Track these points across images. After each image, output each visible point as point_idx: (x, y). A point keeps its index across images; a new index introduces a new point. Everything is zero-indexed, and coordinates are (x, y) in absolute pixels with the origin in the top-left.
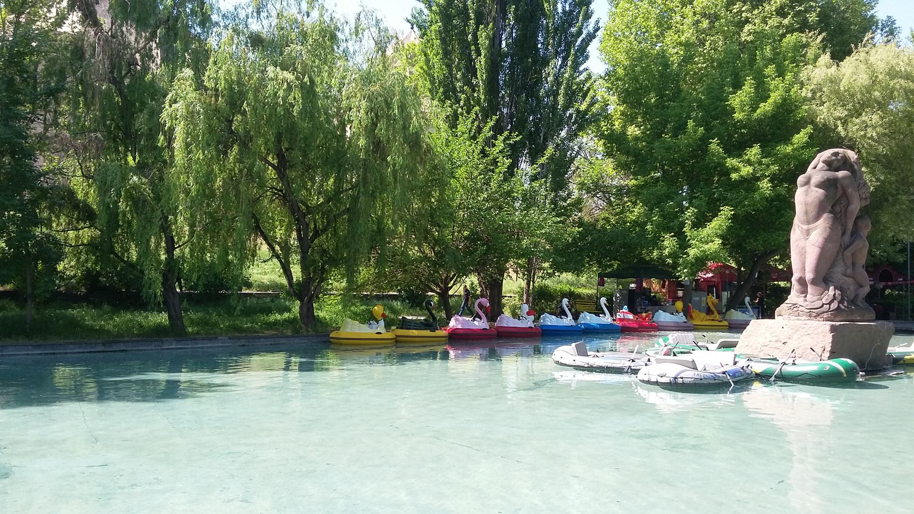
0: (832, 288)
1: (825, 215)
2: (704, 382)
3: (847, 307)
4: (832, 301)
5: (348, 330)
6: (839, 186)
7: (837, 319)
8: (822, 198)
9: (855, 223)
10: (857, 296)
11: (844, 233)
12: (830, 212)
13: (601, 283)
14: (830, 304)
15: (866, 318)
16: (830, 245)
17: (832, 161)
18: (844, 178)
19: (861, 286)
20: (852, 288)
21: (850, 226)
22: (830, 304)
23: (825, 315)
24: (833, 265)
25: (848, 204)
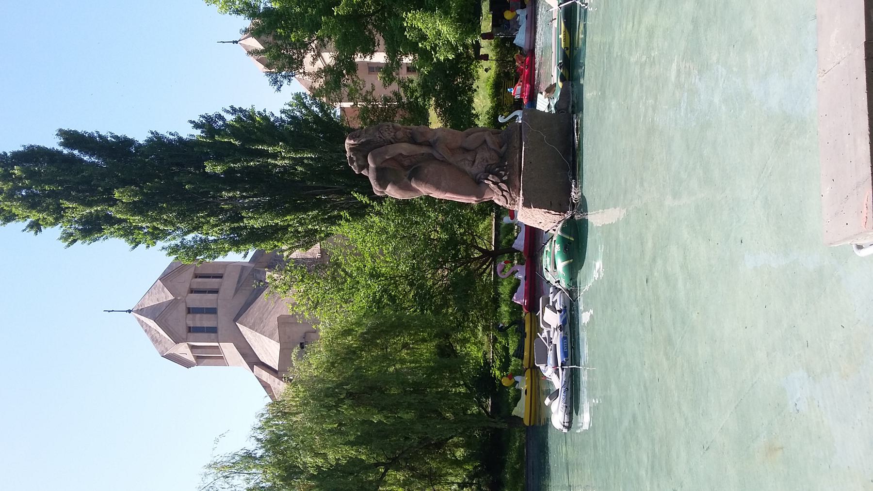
0: (486, 182)
1: (414, 185)
2: (568, 405)
3: (506, 172)
4: (499, 187)
5: (523, 411)
6: (384, 165)
7: (518, 184)
8: (396, 187)
9: (420, 144)
10: (495, 151)
11: (431, 158)
12: (410, 179)
13: (486, 57)
14: (502, 190)
15: (517, 145)
16: (443, 184)
17: (358, 166)
18: (375, 162)
19: (485, 141)
20: (487, 155)
21: (424, 150)
22: (502, 190)
23: (514, 195)
24: (464, 173)
25: (401, 154)
